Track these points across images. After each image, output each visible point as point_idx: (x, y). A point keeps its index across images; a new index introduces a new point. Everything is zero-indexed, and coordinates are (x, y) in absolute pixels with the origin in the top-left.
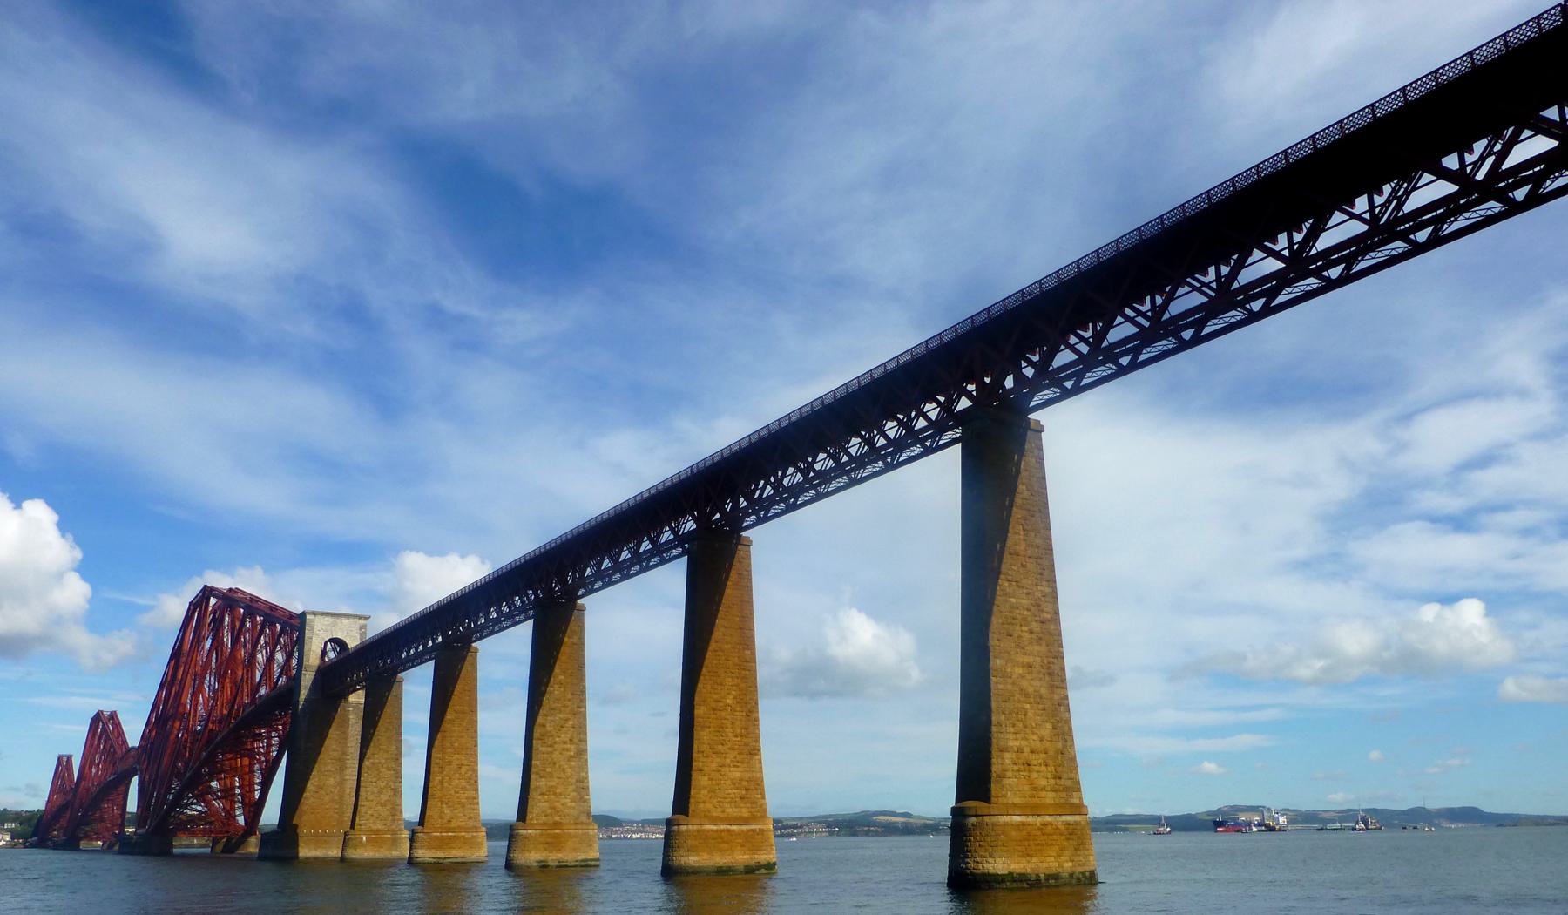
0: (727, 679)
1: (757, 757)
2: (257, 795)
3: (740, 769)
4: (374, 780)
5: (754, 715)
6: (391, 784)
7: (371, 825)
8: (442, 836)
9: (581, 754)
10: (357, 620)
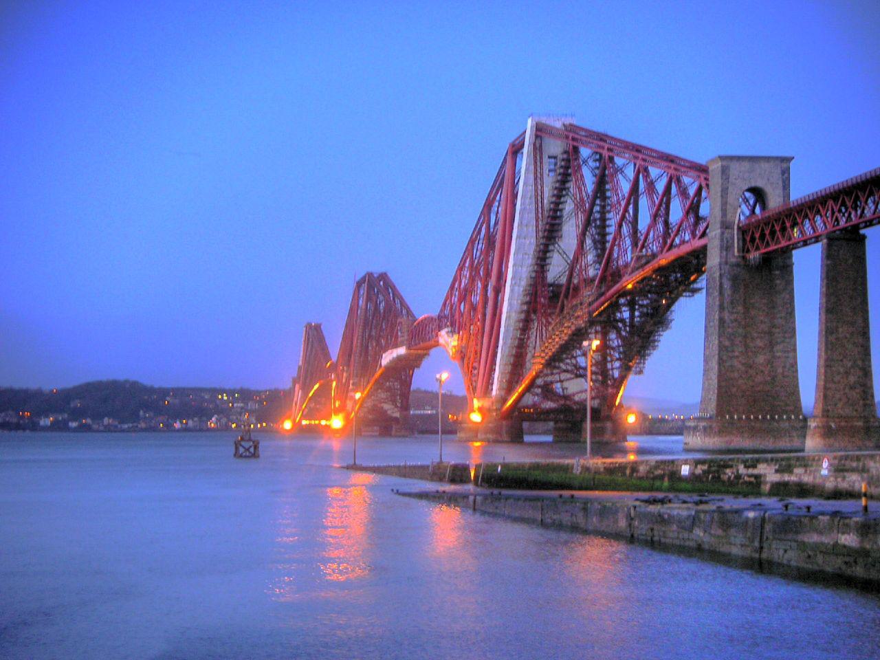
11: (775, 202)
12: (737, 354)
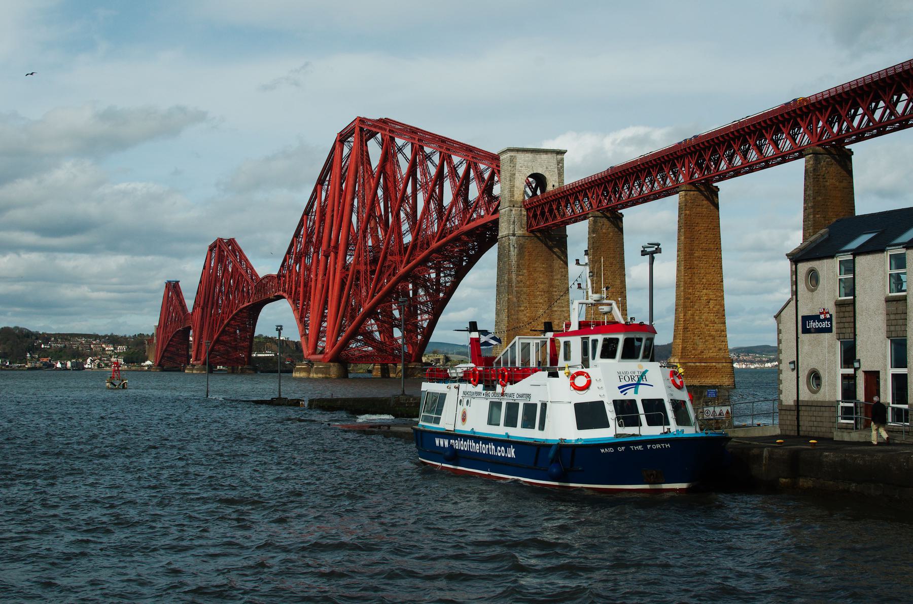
2: (425, 325)
8: (697, 366)
10: (555, 155)
11: (552, 184)
12: (523, 308)
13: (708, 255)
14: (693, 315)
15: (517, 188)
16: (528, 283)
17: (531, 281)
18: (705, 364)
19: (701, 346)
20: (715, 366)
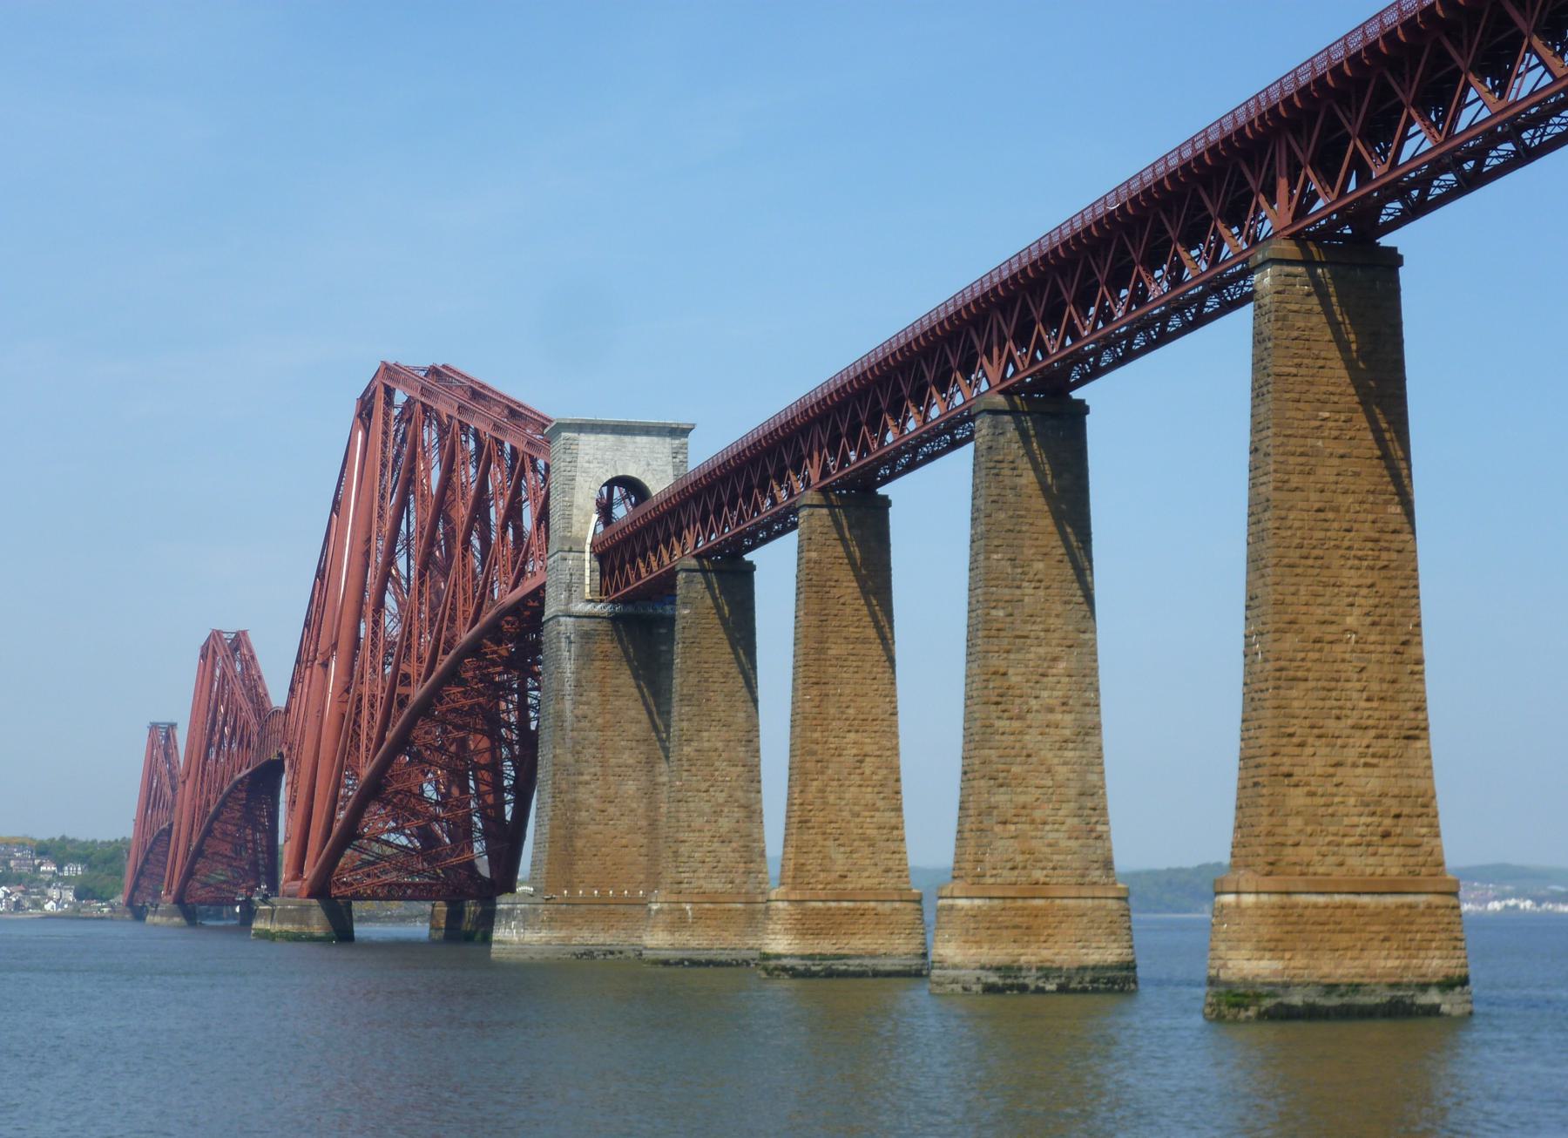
0: (1346, 572)
1: (1419, 744)
3: (1376, 771)
4: (704, 786)
5: (1411, 651)
6: (739, 794)
7: (701, 882)
8: (829, 909)
9: (1087, 734)
12: (587, 778)
13: (863, 652)
14: (822, 791)
15: (579, 508)
16: (600, 721)
17: (608, 716)
18: (851, 905)
19: (840, 861)
20: (874, 909)
